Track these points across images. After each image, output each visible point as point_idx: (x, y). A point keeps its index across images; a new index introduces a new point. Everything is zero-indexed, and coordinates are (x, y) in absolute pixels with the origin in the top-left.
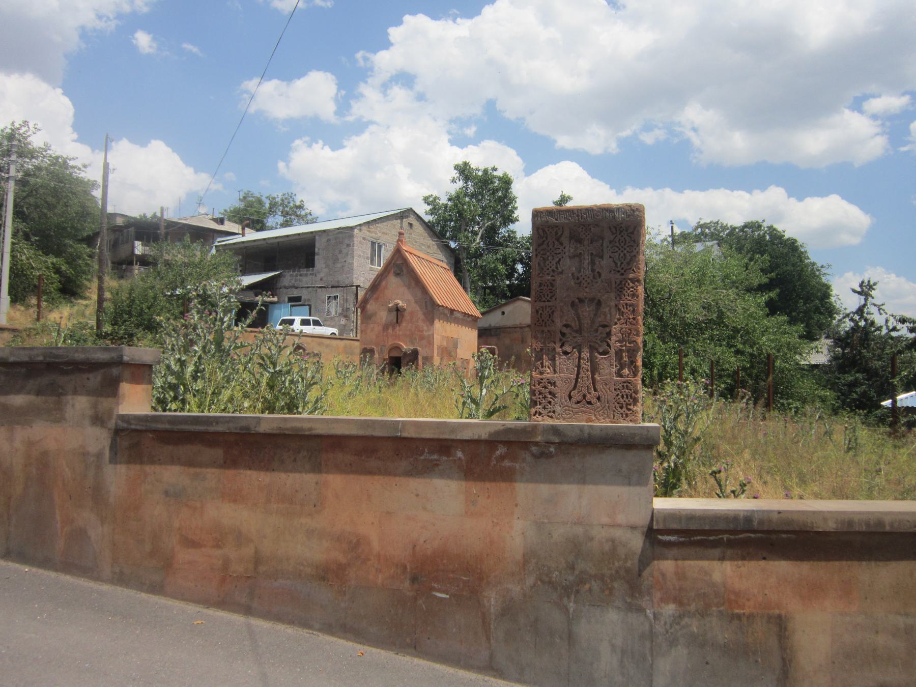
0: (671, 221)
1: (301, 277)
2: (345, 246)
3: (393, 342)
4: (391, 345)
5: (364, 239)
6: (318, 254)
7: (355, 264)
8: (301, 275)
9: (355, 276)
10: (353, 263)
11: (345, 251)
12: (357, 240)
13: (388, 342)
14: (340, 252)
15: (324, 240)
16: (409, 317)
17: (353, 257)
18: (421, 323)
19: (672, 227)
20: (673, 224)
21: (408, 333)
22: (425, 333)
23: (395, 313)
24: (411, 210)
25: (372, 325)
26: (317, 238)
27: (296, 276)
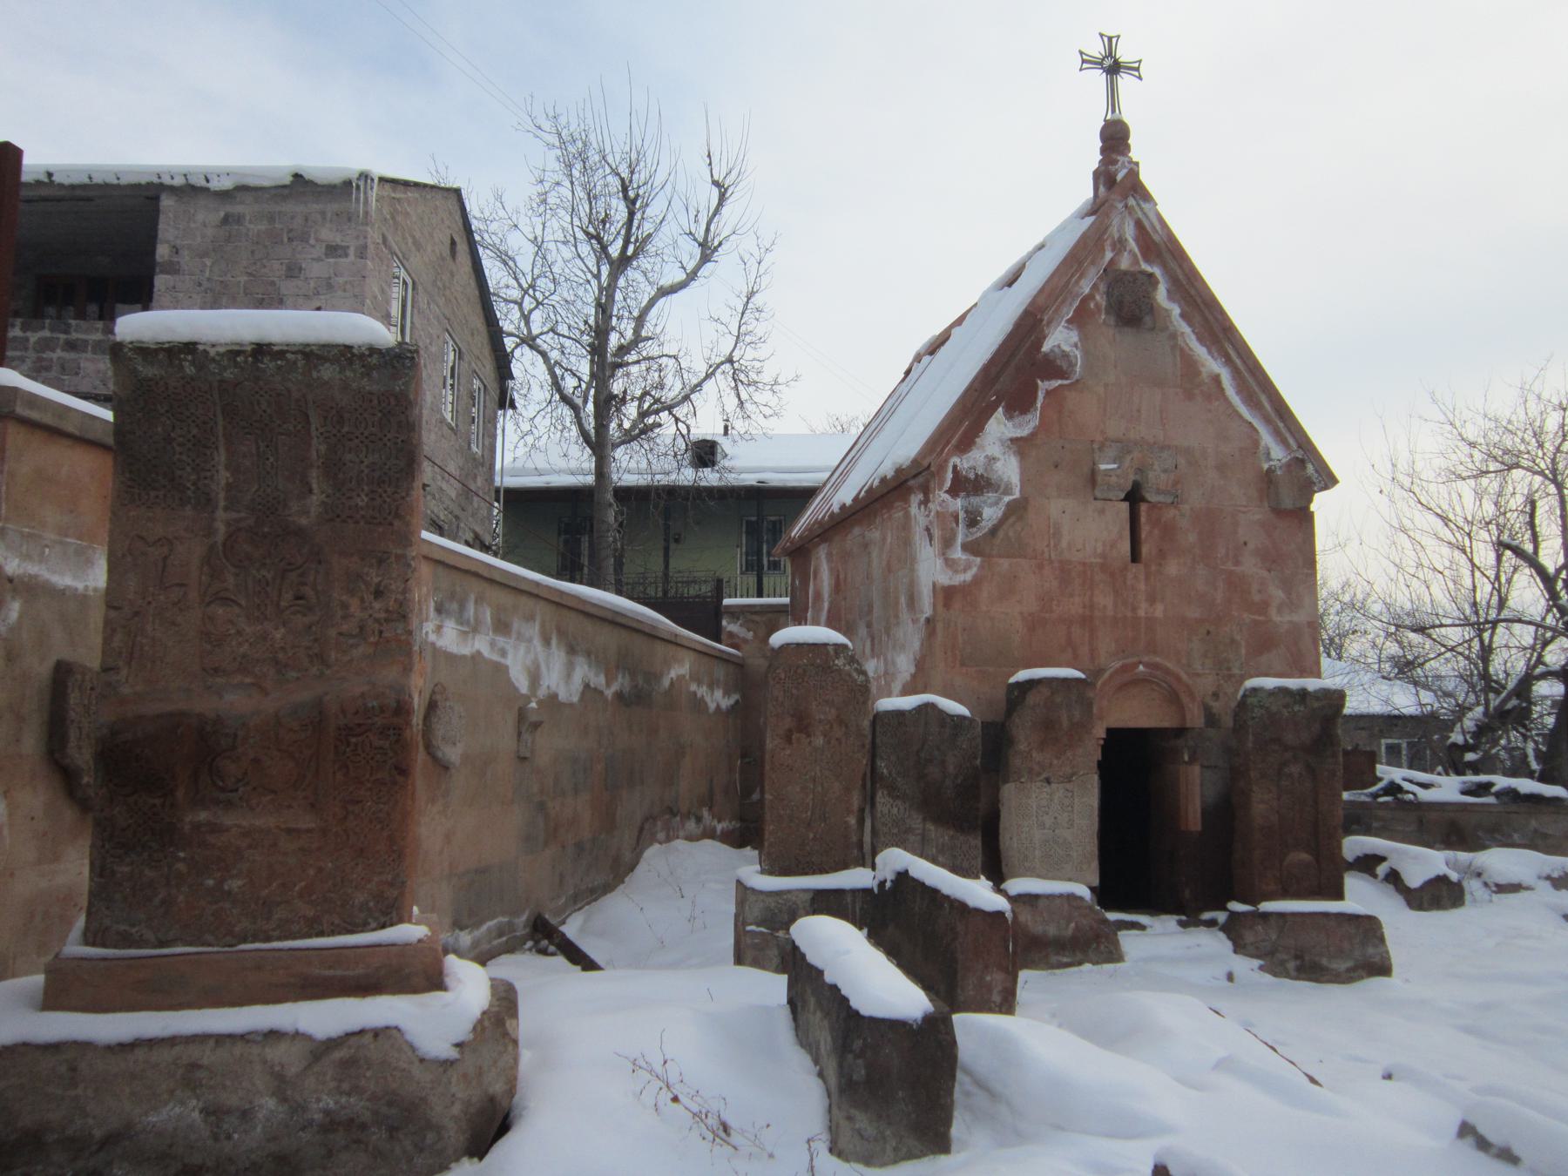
1: (73, 355)
2: (319, 250)
6: (172, 269)
8: (71, 346)
11: (317, 270)
14: (293, 271)
15: (207, 217)
16: (1192, 538)
18: (1250, 566)
21: (1193, 613)
22: (1281, 619)
23: (1125, 505)
24: (457, 192)
25: (1004, 564)
26: (166, 202)
27: (46, 345)
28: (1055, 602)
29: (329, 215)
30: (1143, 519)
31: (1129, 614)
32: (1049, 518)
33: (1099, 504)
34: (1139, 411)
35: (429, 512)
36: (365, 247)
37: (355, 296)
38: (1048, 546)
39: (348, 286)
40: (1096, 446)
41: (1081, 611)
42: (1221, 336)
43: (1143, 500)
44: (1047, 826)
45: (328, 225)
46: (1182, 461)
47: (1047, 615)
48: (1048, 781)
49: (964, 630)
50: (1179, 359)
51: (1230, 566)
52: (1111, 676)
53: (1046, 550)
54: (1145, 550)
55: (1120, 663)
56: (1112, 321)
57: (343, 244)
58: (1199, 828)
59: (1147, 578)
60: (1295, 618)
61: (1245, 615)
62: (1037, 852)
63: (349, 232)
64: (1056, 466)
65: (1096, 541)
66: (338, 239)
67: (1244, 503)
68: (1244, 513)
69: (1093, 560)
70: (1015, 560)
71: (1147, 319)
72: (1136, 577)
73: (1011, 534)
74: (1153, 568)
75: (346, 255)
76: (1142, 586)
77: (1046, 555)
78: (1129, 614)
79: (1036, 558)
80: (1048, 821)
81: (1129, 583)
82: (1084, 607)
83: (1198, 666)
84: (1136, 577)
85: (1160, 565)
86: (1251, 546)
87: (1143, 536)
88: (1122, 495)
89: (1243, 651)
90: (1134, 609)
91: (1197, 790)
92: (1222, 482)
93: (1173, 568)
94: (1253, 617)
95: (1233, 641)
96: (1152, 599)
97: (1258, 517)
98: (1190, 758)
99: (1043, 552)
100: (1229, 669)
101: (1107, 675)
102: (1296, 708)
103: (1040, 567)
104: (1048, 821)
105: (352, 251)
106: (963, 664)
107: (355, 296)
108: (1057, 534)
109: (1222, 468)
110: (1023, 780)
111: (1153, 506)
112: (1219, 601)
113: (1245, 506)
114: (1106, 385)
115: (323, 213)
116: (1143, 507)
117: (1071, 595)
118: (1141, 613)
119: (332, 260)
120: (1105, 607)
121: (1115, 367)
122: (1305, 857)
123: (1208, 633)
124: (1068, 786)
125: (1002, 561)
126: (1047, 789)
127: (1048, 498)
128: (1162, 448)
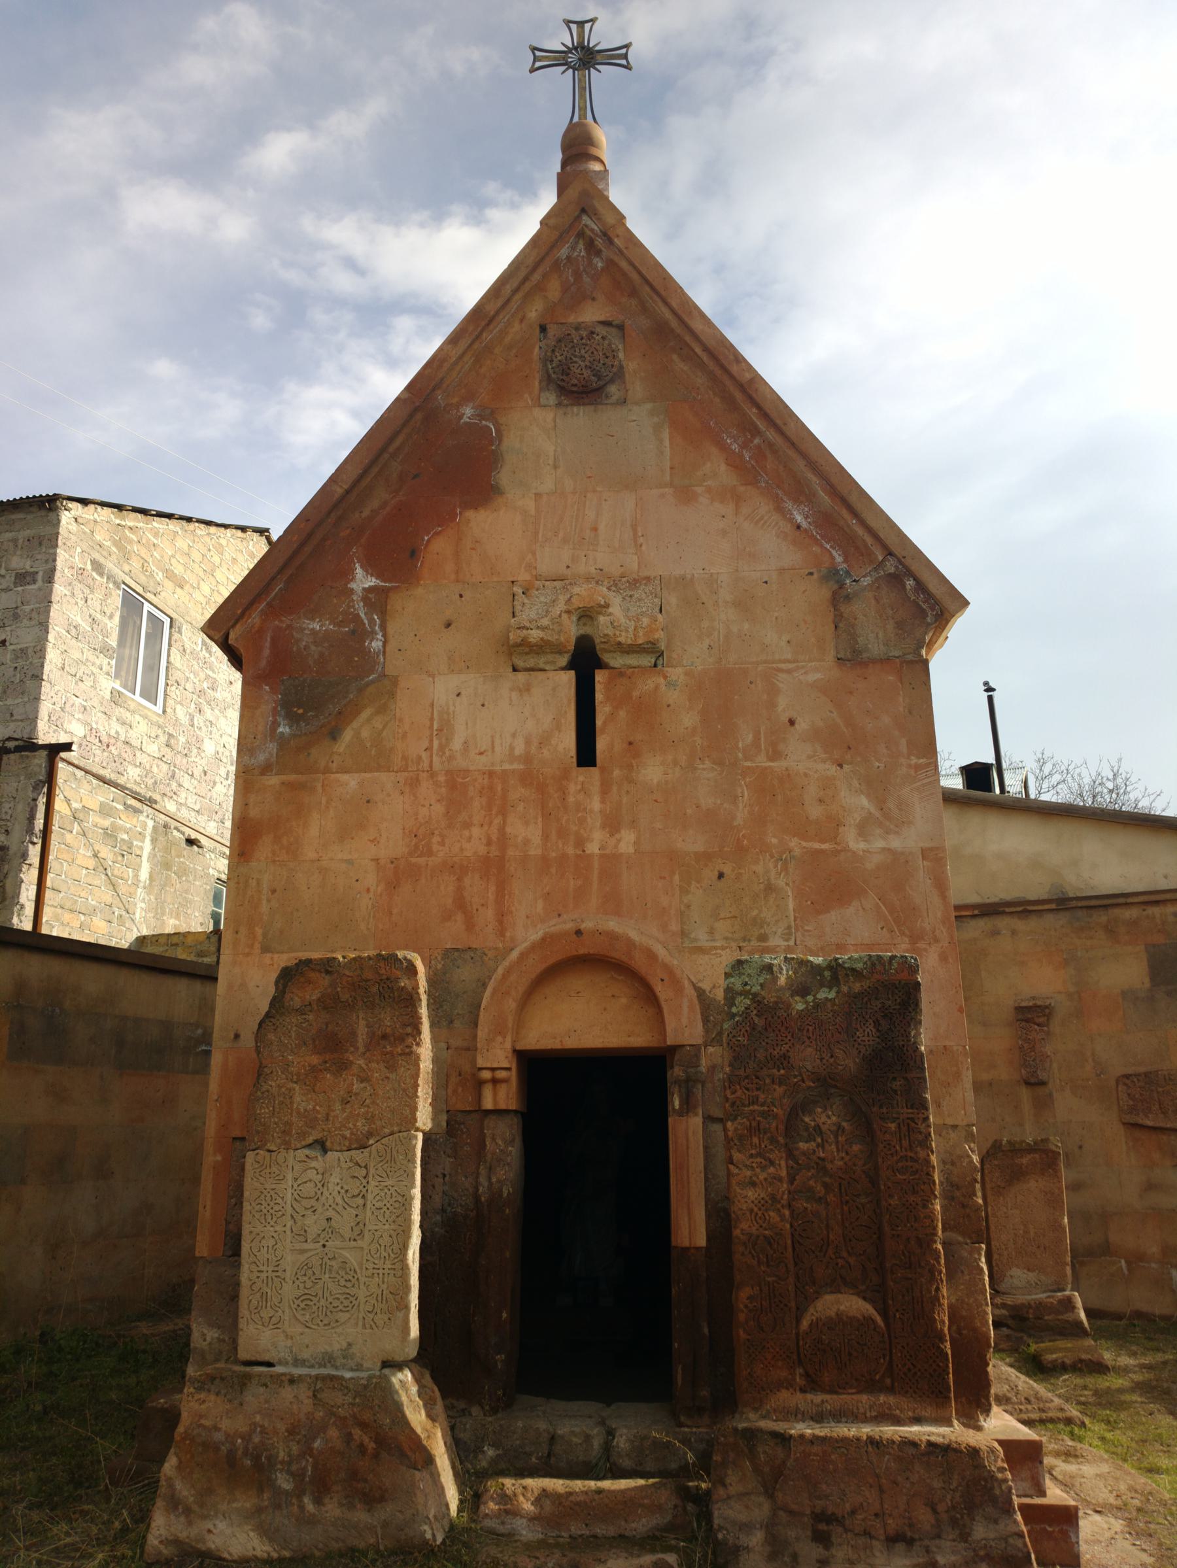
0: (986, 683)
3: (556, 926)
4: (546, 941)
5: (98, 567)
7: (52, 656)
9: (45, 708)
10: (41, 653)
12: (67, 559)
13: (502, 916)
16: (689, 720)
17: (44, 626)
19: (990, 699)
20: (993, 690)
21: (692, 842)
23: (568, 679)
25: (351, 782)
28: (436, 839)
29: (21, 541)
30: (599, 697)
31: (571, 851)
32: (432, 705)
33: (521, 677)
34: (595, 529)
35: (211, 871)
36: (53, 570)
37: (40, 623)
38: (429, 749)
39: (34, 615)
40: (518, 590)
41: (482, 850)
42: (738, 396)
43: (601, 665)
44: (310, 1238)
45: (19, 553)
46: (672, 600)
47: (422, 861)
48: (322, 1146)
49: (274, 891)
50: (667, 443)
51: (762, 761)
52: (523, 956)
53: (424, 755)
54: (601, 744)
55: (540, 934)
56: (551, 398)
57: (32, 570)
58: (701, 1241)
59: (605, 791)
60: (895, 843)
61: (794, 843)
62: (288, 1287)
63: (39, 557)
64: (448, 625)
65: (514, 735)
66: (27, 565)
67: (789, 657)
68: (789, 672)
69: (507, 766)
70: (368, 775)
71: (613, 389)
72: (584, 790)
73: (365, 734)
74: (617, 773)
75: (34, 581)
76: (596, 805)
77: (426, 765)
78: (571, 851)
79: (405, 769)
80: (313, 1224)
81: (571, 799)
82: (489, 843)
83: (701, 936)
84: (584, 790)
85: (630, 767)
86: (802, 725)
87: (599, 722)
88: (564, 660)
89: (791, 905)
90: (580, 843)
91: (697, 1162)
92: (746, 626)
93: (653, 771)
94: (804, 844)
95: (770, 888)
96: (612, 824)
97: (818, 676)
98: (680, 1104)
99: (420, 758)
100: (763, 938)
101: (514, 955)
102: (823, 994)
103: (414, 783)
104: (313, 1224)
105: (40, 577)
106: (266, 949)
107: (40, 623)
108: (445, 728)
109: (744, 604)
110: (273, 1148)
111: (620, 673)
112: (739, 821)
113: (789, 661)
114: (538, 496)
115: (15, 541)
116: (600, 677)
117: (467, 825)
118: (593, 848)
119: (20, 589)
120: (527, 842)
121: (555, 467)
122: (853, 1305)
123: (721, 876)
124: (357, 1155)
125: (344, 777)
126: (319, 1162)
127: (433, 677)
128: (634, 583)
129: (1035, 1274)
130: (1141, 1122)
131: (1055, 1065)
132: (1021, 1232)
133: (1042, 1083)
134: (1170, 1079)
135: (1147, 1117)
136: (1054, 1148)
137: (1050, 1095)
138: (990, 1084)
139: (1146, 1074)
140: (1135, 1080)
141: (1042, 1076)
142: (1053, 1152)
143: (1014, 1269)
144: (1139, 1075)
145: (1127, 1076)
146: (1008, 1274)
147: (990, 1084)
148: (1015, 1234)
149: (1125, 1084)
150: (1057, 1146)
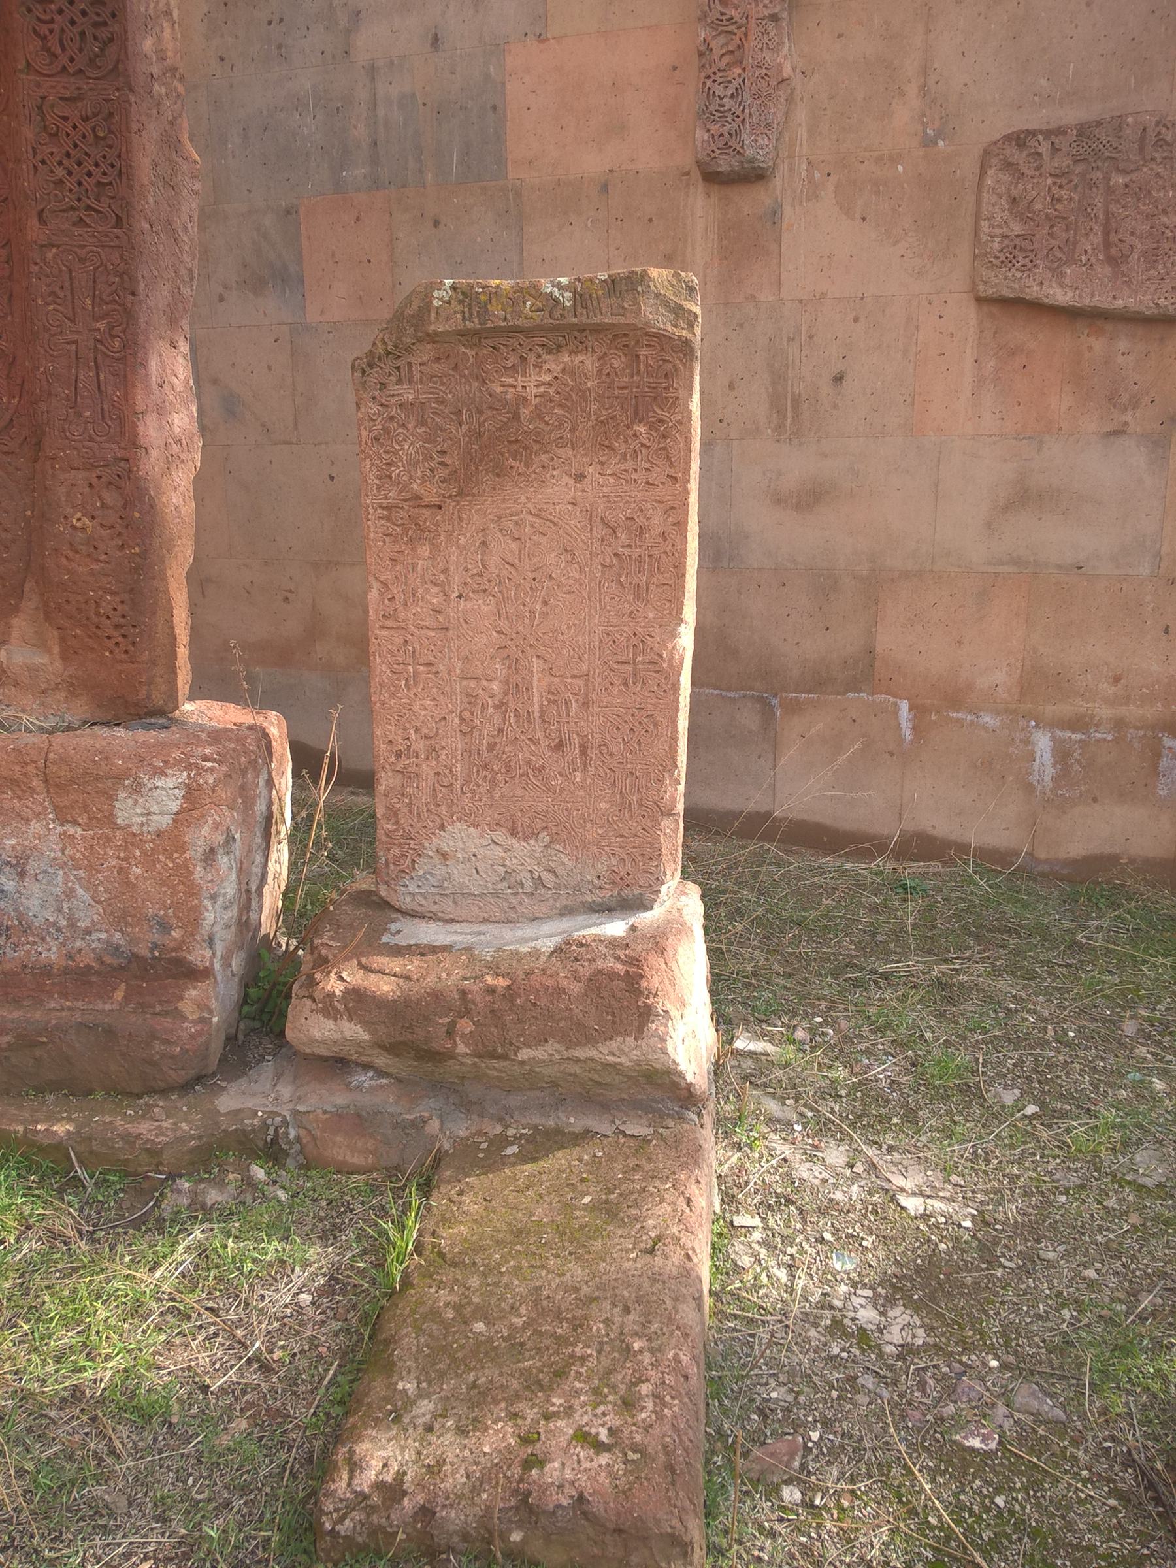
129: (536, 846)
130: (1034, 292)
131: (801, 115)
132: (495, 687)
133: (754, 176)
134: (1161, 142)
135: (1059, 276)
136: (662, 321)
137: (774, 216)
138: (605, 188)
139: (1084, 131)
140: (1045, 149)
141: (756, 147)
142: (660, 339)
143: (458, 828)
144: (1061, 131)
145: (1020, 139)
146: (430, 848)
147: (605, 188)
148: (472, 699)
149: (1008, 165)
150: (678, 311)
